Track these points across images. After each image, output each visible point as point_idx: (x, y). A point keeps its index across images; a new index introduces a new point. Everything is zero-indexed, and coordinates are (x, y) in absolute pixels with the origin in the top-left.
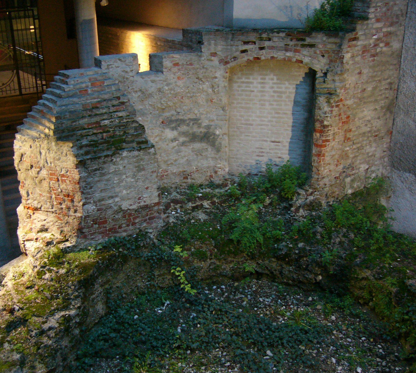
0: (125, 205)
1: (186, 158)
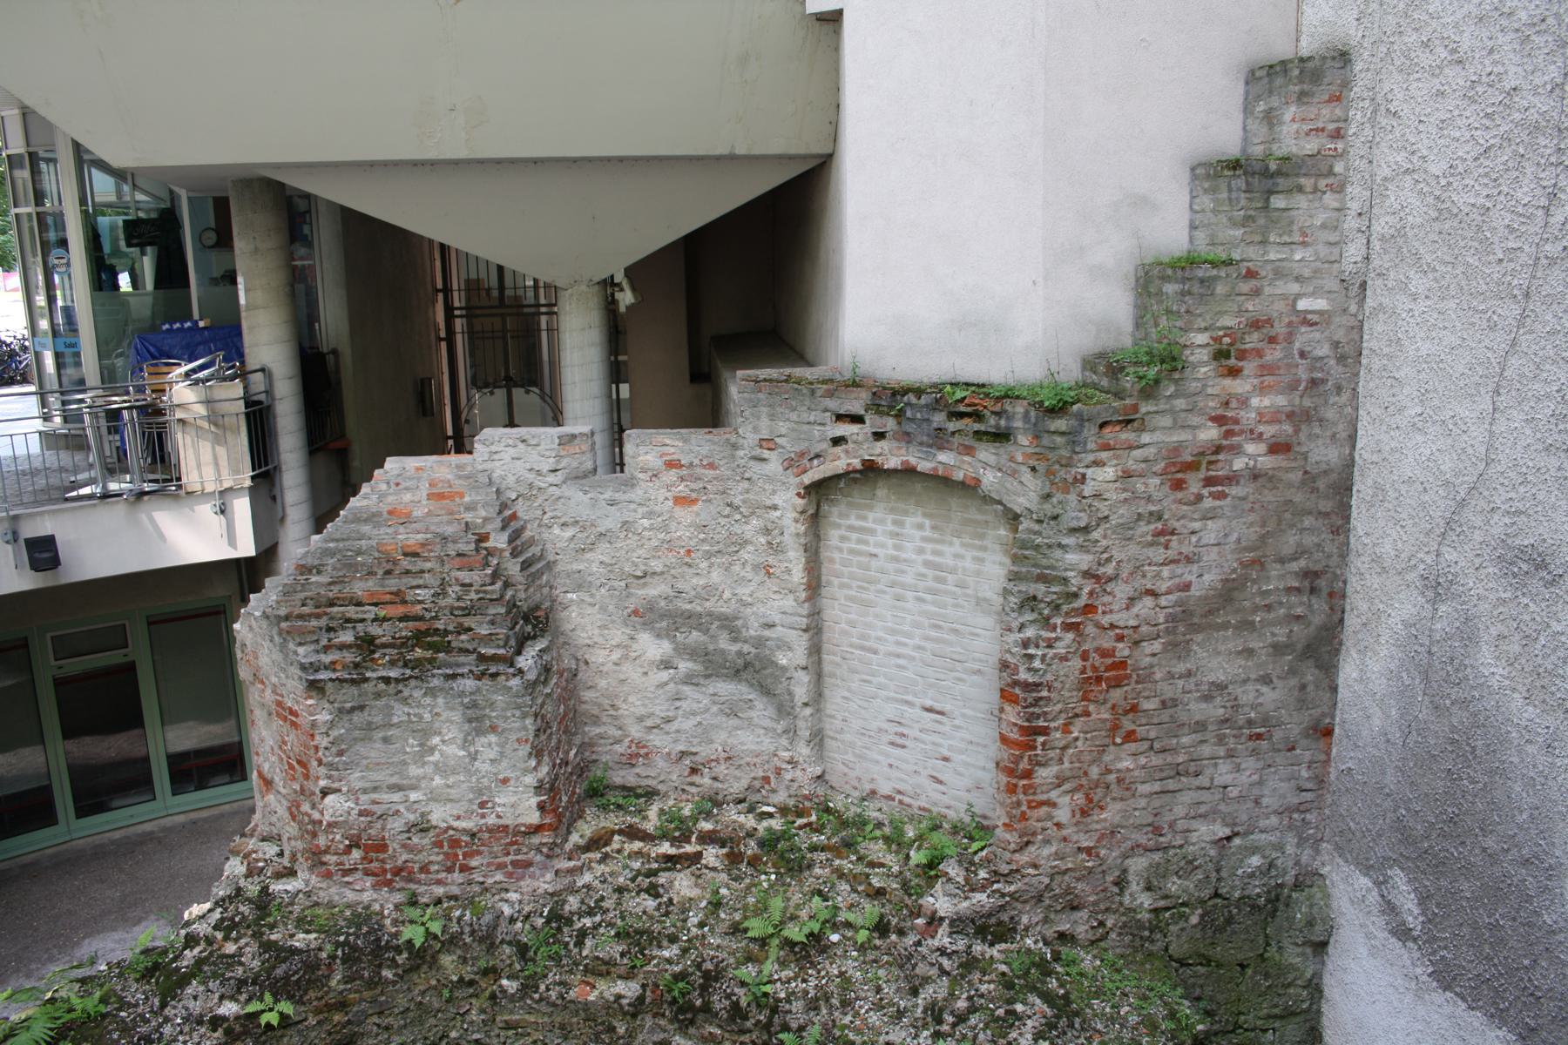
0: (439, 815)
1: (698, 719)
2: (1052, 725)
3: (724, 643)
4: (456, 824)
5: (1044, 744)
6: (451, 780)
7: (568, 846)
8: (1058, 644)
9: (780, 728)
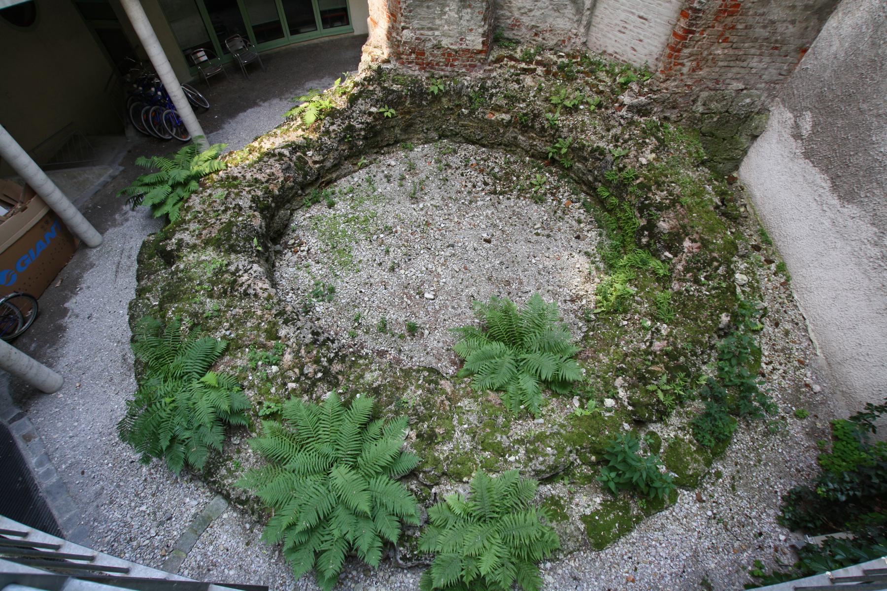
0: (445, 42)
7: (489, 60)
9: (575, 19)
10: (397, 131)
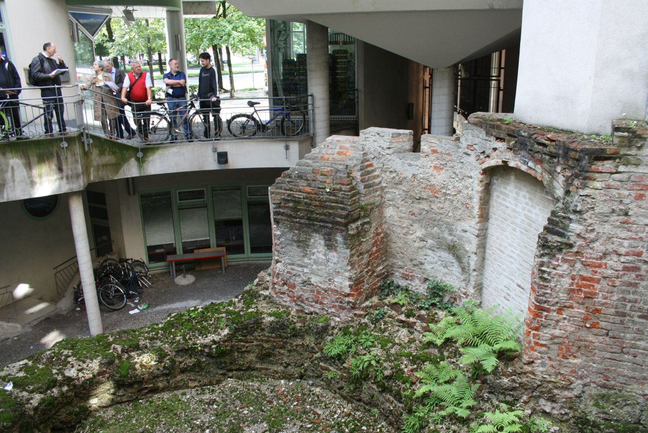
0: (314, 280)
1: (433, 266)
2: (552, 308)
3: (446, 235)
4: (320, 285)
5: (546, 316)
6: (320, 267)
7: (364, 305)
8: (559, 268)
9: (462, 278)
10: (252, 357)
